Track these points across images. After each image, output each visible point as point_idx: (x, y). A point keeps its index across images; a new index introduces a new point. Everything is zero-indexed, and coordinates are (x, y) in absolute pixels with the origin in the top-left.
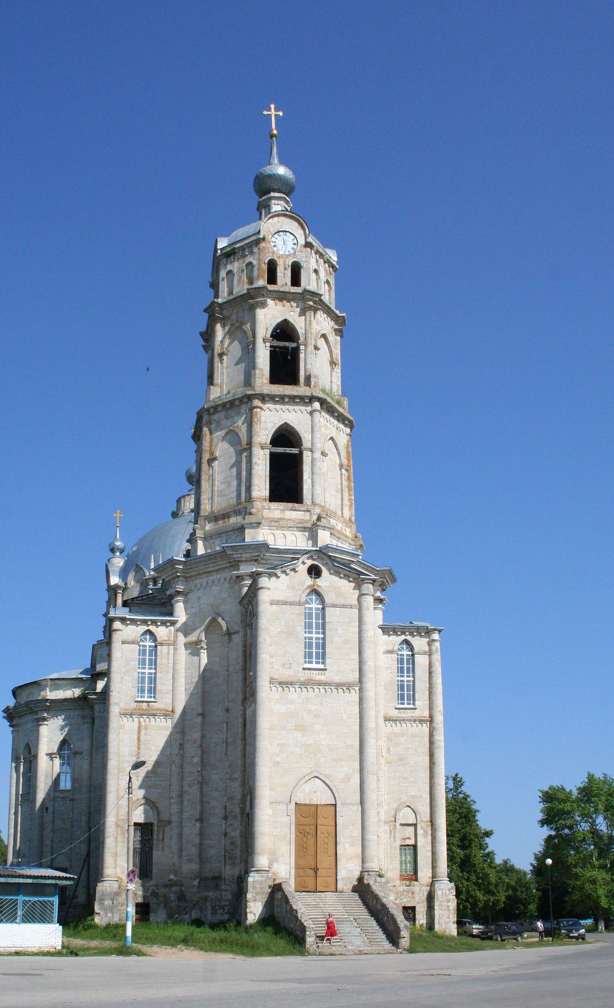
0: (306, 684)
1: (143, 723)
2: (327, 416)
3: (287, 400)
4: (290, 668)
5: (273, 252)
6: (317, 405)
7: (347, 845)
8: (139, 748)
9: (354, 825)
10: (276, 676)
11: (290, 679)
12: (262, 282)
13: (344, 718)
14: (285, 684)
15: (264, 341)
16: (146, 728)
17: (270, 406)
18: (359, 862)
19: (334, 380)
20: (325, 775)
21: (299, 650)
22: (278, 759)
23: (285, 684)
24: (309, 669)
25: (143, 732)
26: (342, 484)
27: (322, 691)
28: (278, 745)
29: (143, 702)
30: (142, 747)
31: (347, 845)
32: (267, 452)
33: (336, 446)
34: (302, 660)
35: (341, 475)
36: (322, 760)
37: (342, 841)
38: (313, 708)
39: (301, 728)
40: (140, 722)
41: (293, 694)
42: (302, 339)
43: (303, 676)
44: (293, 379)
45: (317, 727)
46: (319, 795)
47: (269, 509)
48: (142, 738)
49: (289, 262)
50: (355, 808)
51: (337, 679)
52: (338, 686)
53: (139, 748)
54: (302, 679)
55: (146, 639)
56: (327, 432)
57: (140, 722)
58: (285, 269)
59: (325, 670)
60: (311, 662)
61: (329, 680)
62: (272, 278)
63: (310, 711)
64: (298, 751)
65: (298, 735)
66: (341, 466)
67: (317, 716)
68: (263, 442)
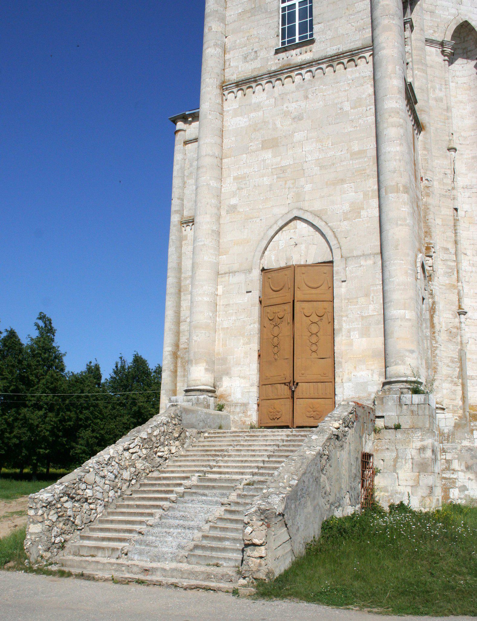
4: (256, 58)
7: (355, 335)
9: (367, 295)
11: (255, 74)
13: (347, 107)
18: (378, 365)
22: (233, 201)
28: (235, 178)
31: (355, 335)
37: (345, 326)
38: (292, 107)
39: (271, 144)
41: (260, 95)
45: (298, 136)
46: (300, 248)
50: (370, 262)
51: (331, 51)
54: (274, 68)
63: (286, 114)
64: (266, 181)
65: (268, 155)
67: (299, 118)
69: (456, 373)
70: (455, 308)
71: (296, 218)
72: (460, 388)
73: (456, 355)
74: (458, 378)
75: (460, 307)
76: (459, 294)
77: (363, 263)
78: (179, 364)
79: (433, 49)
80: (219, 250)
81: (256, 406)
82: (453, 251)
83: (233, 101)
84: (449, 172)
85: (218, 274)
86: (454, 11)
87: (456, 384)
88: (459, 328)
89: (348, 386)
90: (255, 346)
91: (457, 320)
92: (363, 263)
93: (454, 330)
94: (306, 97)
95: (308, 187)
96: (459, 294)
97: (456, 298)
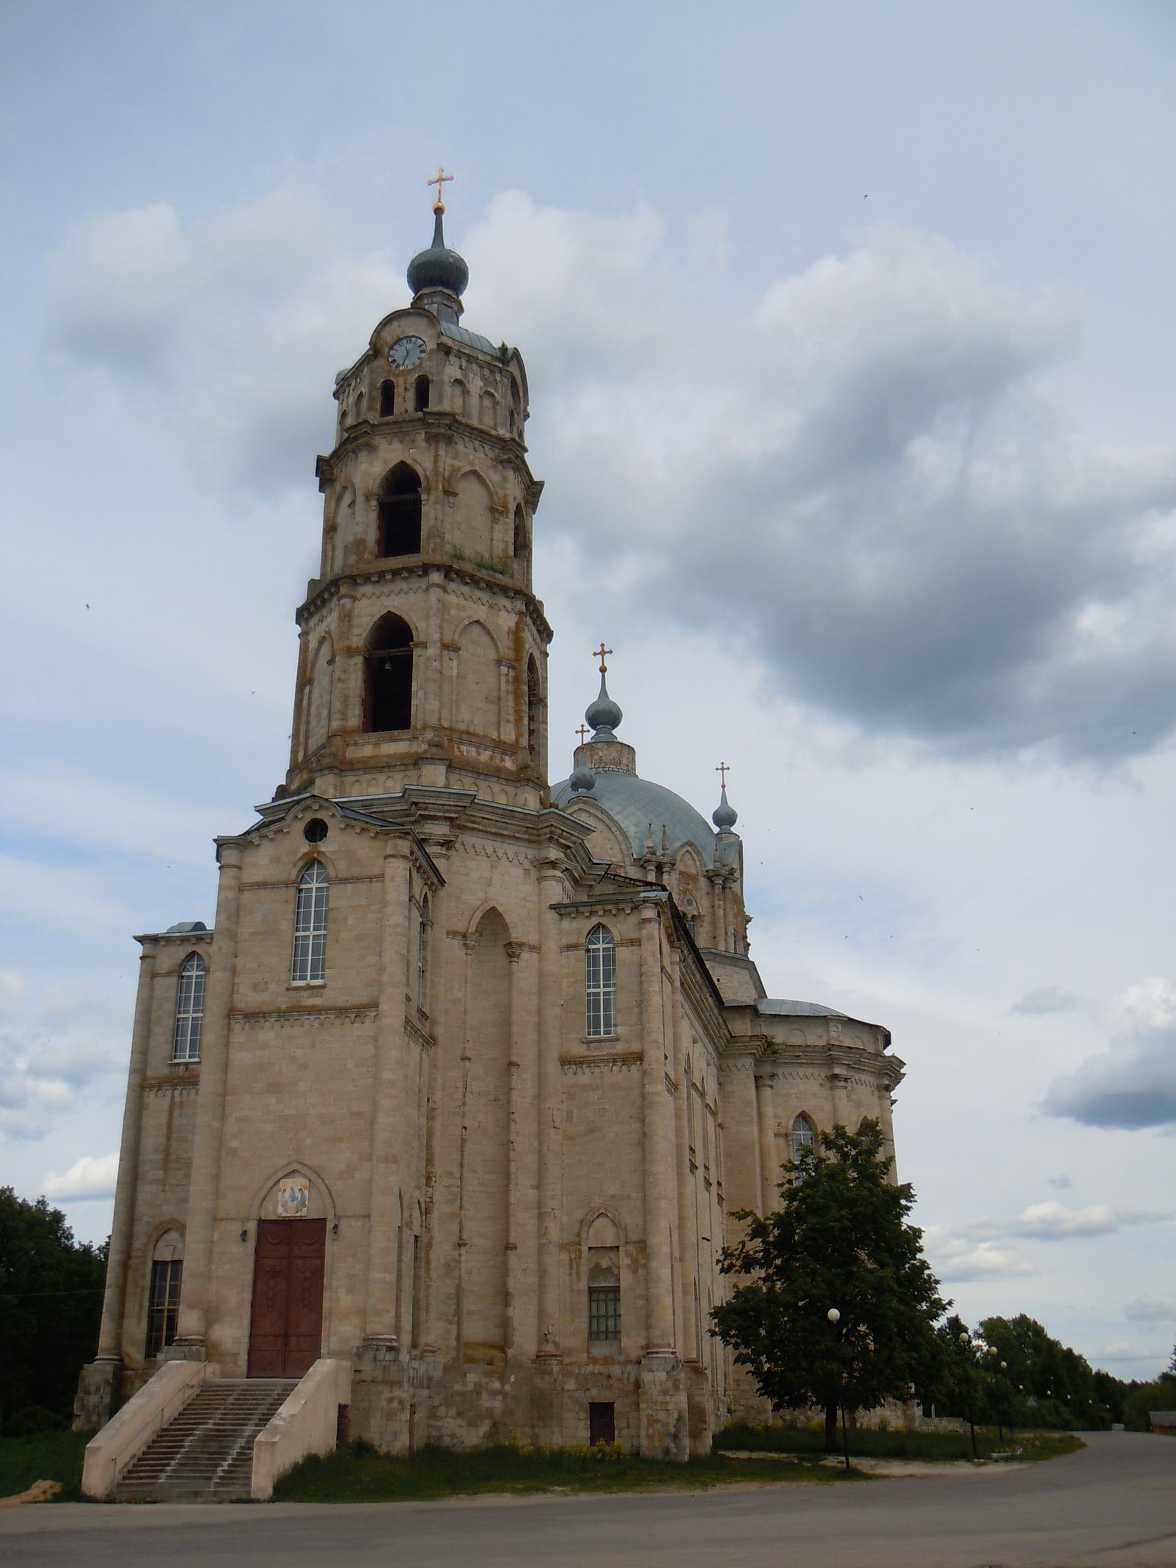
0: (286, 1014)
1: (177, 1099)
2: (466, 590)
3: (388, 577)
4: (266, 990)
5: (389, 371)
6: (436, 577)
8: (169, 1138)
10: (242, 1006)
11: (264, 1008)
12: (374, 417)
14: (254, 1016)
15: (368, 497)
16: (182, 1105)
17: (366, 589)
19: (497, 536)
20: (310, 1167)
21: (278, 959)
22: (234, 1144)
23: (254, 1016)
24: (297, 989)
25: (176, 1113)
26: (499, 690)
27: (317, 1024)
29: (179, 1064)
30: (175, 1135)
32: (359, 660)
33: (488, 632)
34: (285, 976)
35: (500, 675)
36: (309, 1141)
37: (335, 1283)
39: (275, 1088)
40: (173, 1097)
41: (268, 1033)
42: (424, 484)
43: (283, 1002)
44: (413, 545)
45: (302, 1086)
47: (356, 744)
48: (176, 1123)
49: (412, 379)
51: (341, 1001)
52: (342, 1011)
53: (169, 1138)
54: (283, 1007)
55: (192, 966)
56: (463, 614)
57: (173, 1097)
58: (406, 389)
59: (323, 987)
60: (303, 978)
61: (326, 1003)
62: (387, 407)
65: (271, 1100)
66: (499, 663)
68: (354, 645)
69: (452, 1311)
70: (455, 1239)
71: (294, 1171)
72: (455, 1327)
73: (453, 1291)
74: (454, 1316)
75: (461, 1238)
76: (460, 1223)
77: (353, 1223)
78: (130, 1278)
79: (455, 942)
80: (217, 1194)
81: (246, 1357)
82: (457, 1175)
83: (240, 1033)
84: (461, 1085)
85: (215, 1219)
86: (481, 895)
87: (451, 1323)
88: (458, 1261)
89: (333, 1339)
90: (248, 1296)
91: (457, 1252)
92: (353, 1223)
93: (453, 1264)
94: (313, 1046)
95: (309, 1141)
96: (460, 1223)
97: (456, 1228)
